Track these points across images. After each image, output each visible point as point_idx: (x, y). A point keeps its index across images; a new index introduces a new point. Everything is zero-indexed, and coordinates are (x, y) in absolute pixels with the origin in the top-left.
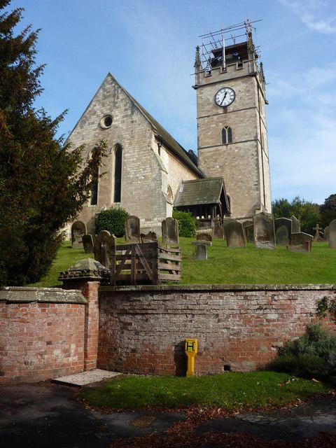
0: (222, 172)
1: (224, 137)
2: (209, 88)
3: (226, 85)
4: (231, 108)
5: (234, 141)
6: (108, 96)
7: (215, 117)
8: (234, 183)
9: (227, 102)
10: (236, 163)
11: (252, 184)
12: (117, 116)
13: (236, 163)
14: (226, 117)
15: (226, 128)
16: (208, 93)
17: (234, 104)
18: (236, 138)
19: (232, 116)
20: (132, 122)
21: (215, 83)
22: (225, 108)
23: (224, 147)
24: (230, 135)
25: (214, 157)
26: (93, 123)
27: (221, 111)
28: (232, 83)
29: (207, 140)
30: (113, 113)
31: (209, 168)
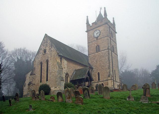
0: (97, 63)
1: (97, 49)
2: (91, 31)
3: (97, 29)
4: (99, 38)
5: (100, 50)
6: (45, 42)
7: (94, 42)
8: (101, 67)
9: (96, 35)
10: (101, 59)
11: (107, 67)
12: (47, 49)
13: (101, 59)
14: (97, 41)
15: (97, 46)
16: (91, 32)
17: (100, 36)
18: (101, 49)
19: (99, 41)
20: (51, 51)
21: (93, 29)
22: (97, 38)
23: (97, 53)
24: (99, 48)
25: (94, 58)
26: (41, 53)
27: (95, 39)
28: (99, 28)
29: (91, 51)
30: (46, 49)
31: (92, 62)
